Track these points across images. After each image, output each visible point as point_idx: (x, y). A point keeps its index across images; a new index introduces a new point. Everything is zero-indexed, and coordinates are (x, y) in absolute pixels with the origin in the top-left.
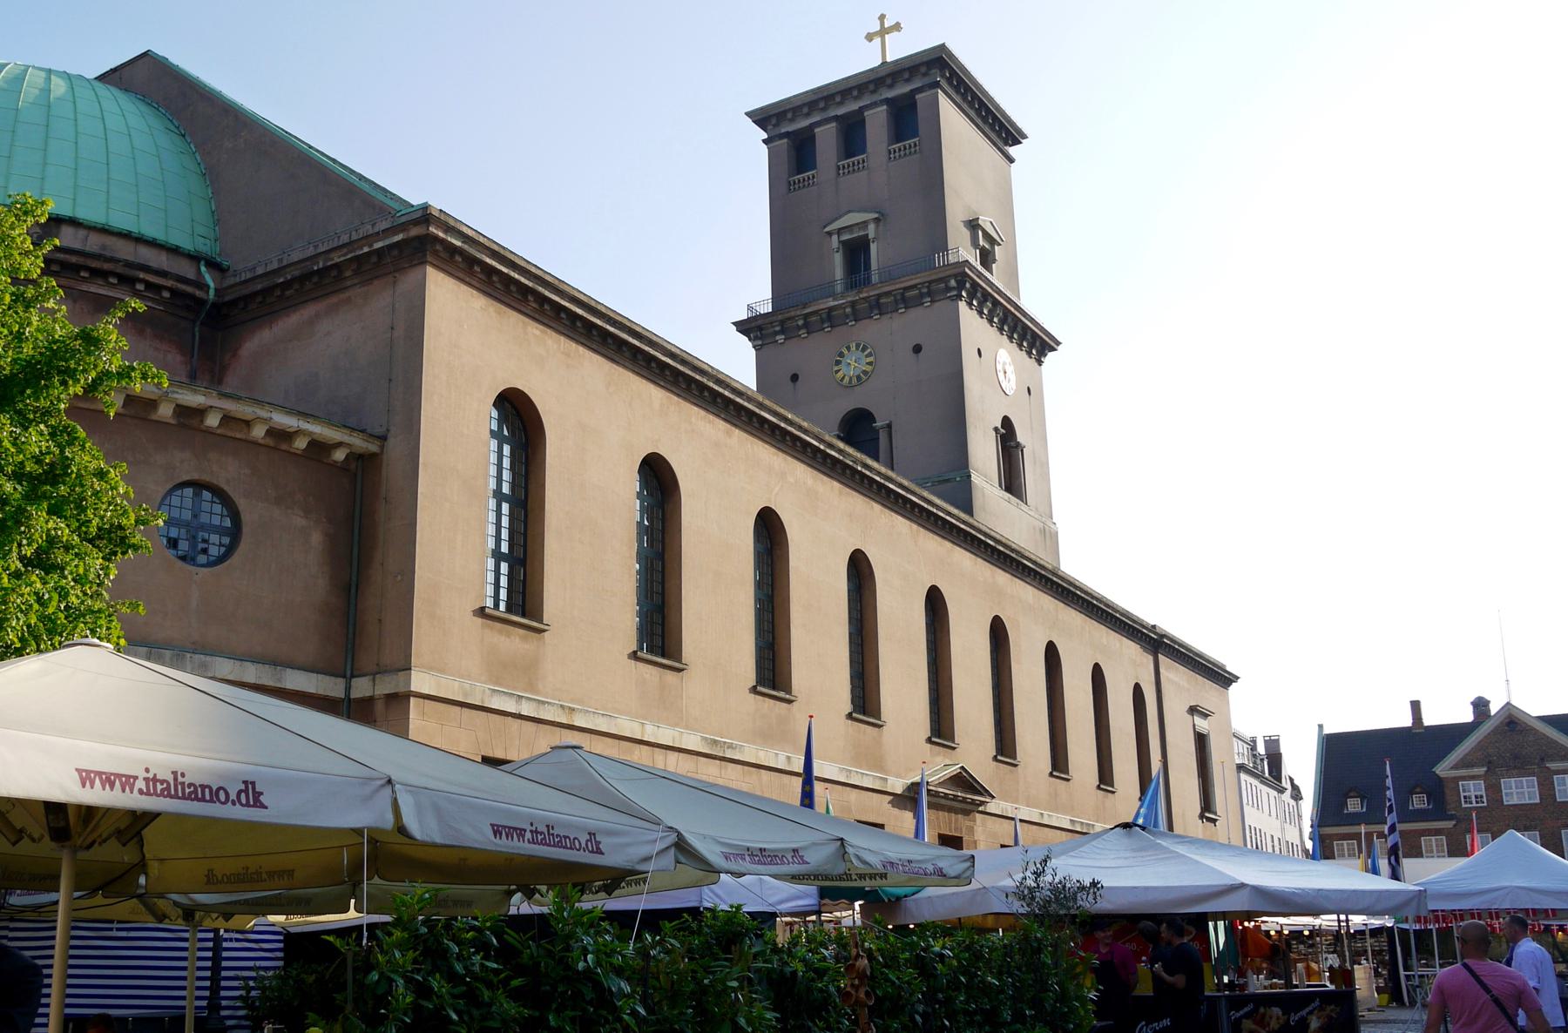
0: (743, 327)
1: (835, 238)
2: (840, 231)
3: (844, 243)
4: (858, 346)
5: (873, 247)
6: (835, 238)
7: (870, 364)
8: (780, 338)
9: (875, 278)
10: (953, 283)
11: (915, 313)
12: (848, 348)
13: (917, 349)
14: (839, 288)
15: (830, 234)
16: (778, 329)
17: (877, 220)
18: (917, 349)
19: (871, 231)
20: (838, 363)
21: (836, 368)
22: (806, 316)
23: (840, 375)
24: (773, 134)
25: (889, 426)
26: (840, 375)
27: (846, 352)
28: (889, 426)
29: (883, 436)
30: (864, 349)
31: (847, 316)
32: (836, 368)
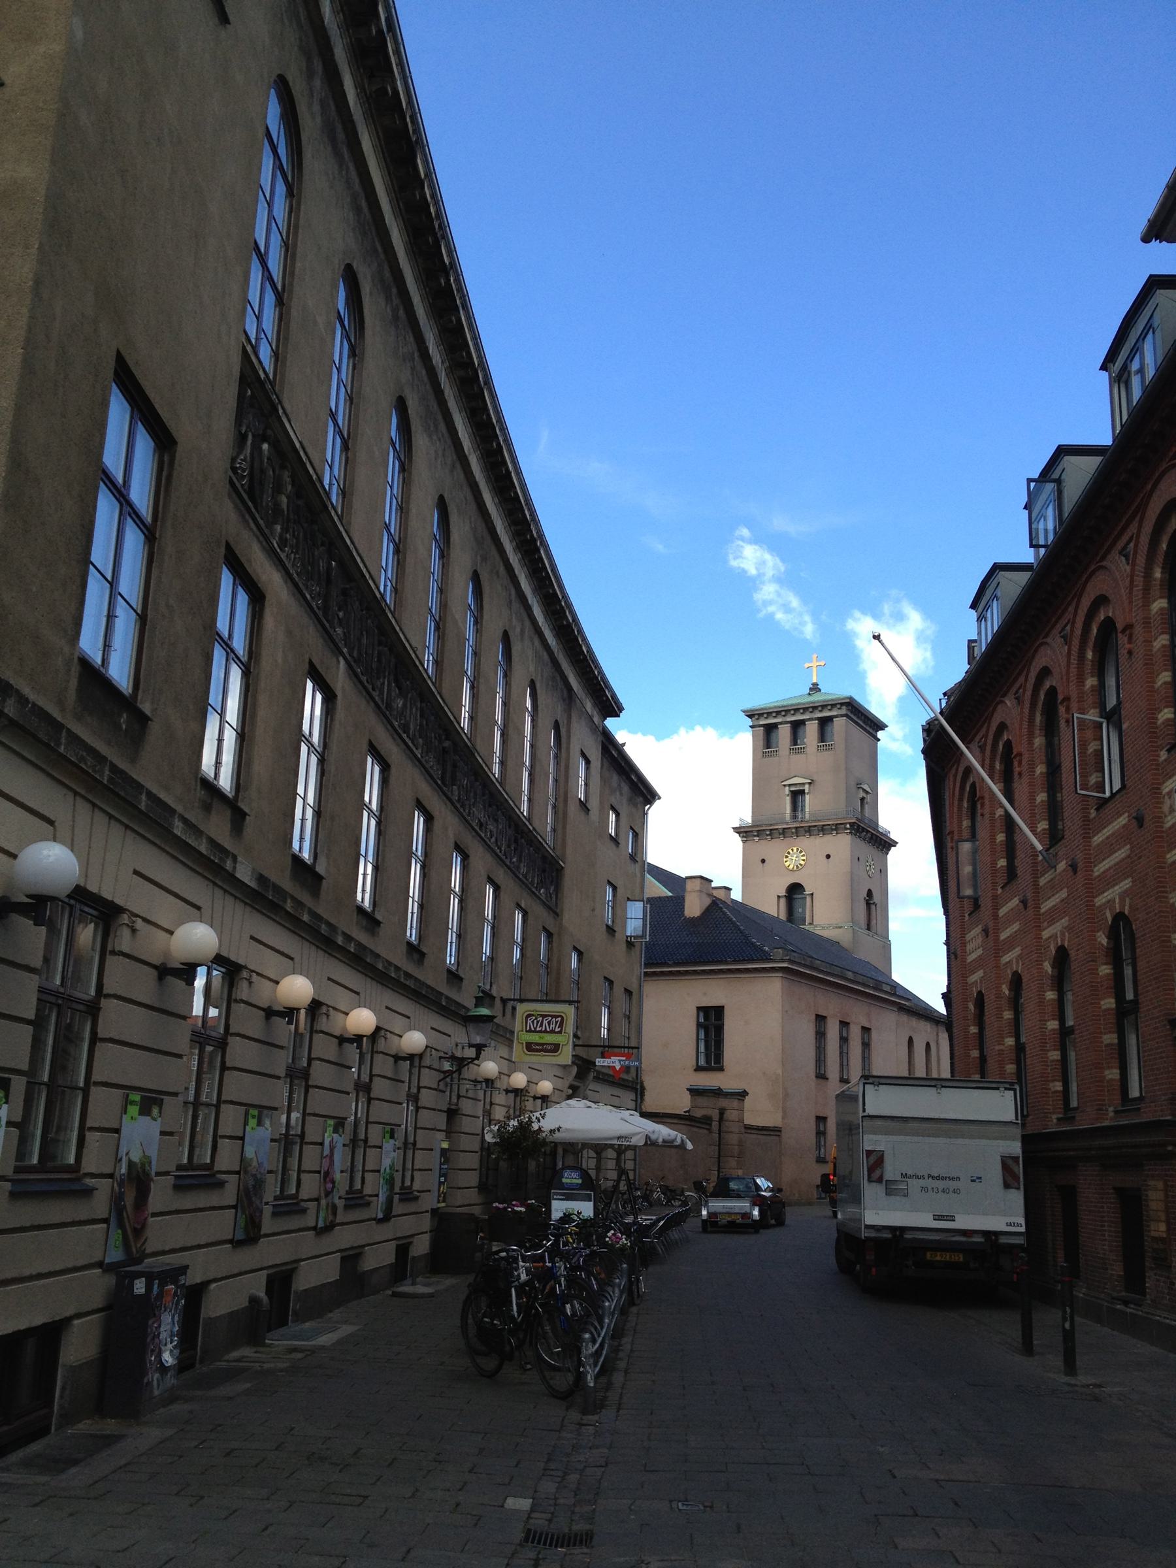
0: (738, 830)
1: (787, 788)
2: (790, 785)
3: (792, 792)
4: (798, 849)
5: (807, 797)
6: (787, 788)
7: (804, 860)
8: (756, 839)
9: (807, 816)
10: (848, 826)
11: (828, 838)
12: (792, 850)
13: (828, 857)
14: (788, 817)
15: (784, 785)
16: (755, 834)
17: (810, 783)
18: (828, 857)
19: (806, 788)
20: (787, 857)
21: (785, 860)
22: (771, 830)
23: (787, 864)
24: (756, 723)
25: (812, 894)
26: (787, 864)
27: (791, 852)
28: (812, 894)
29: (808, 899)
30: (801, 852)
31: (793, 833)
32: (785, 860)
